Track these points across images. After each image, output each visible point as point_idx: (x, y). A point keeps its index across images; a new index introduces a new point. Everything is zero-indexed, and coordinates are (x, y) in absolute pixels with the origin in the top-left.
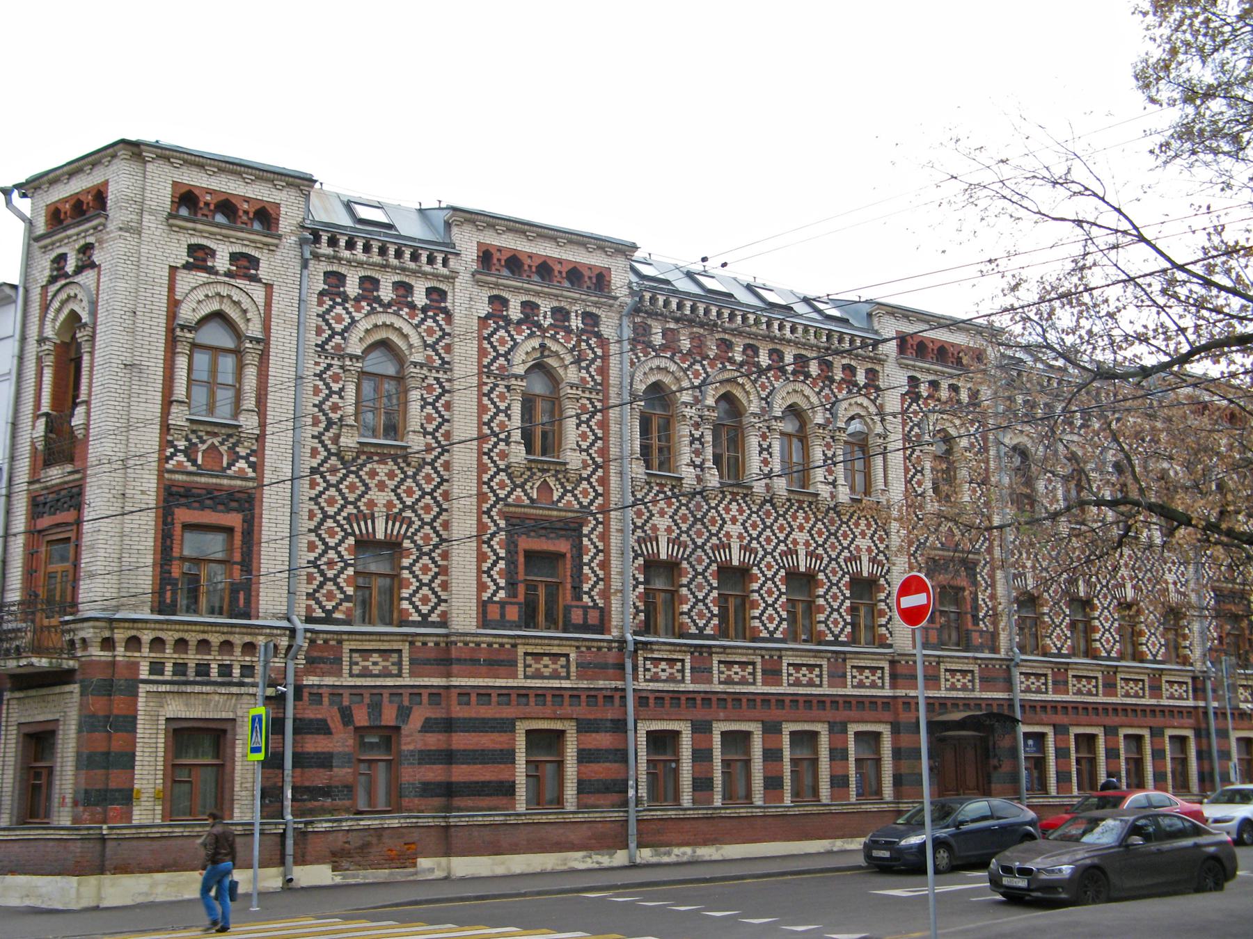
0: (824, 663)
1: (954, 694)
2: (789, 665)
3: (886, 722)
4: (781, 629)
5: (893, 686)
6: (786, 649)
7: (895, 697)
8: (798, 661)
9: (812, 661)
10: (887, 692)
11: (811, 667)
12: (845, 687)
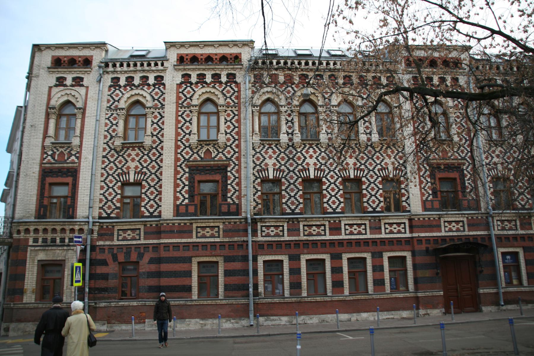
0: (367, 222)
1: (451, 234)
2: (345, 225)
3: (408, 251)
4: (340, 207)
5: (411, 232)
6: (342, 217)
7: (412, 238)
8: (351, 222)
9: (359, 222)
10: (408, 235)
11: (359, 225)
12: (381, 233)
